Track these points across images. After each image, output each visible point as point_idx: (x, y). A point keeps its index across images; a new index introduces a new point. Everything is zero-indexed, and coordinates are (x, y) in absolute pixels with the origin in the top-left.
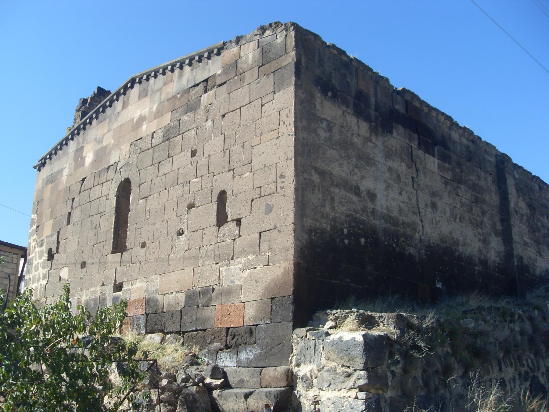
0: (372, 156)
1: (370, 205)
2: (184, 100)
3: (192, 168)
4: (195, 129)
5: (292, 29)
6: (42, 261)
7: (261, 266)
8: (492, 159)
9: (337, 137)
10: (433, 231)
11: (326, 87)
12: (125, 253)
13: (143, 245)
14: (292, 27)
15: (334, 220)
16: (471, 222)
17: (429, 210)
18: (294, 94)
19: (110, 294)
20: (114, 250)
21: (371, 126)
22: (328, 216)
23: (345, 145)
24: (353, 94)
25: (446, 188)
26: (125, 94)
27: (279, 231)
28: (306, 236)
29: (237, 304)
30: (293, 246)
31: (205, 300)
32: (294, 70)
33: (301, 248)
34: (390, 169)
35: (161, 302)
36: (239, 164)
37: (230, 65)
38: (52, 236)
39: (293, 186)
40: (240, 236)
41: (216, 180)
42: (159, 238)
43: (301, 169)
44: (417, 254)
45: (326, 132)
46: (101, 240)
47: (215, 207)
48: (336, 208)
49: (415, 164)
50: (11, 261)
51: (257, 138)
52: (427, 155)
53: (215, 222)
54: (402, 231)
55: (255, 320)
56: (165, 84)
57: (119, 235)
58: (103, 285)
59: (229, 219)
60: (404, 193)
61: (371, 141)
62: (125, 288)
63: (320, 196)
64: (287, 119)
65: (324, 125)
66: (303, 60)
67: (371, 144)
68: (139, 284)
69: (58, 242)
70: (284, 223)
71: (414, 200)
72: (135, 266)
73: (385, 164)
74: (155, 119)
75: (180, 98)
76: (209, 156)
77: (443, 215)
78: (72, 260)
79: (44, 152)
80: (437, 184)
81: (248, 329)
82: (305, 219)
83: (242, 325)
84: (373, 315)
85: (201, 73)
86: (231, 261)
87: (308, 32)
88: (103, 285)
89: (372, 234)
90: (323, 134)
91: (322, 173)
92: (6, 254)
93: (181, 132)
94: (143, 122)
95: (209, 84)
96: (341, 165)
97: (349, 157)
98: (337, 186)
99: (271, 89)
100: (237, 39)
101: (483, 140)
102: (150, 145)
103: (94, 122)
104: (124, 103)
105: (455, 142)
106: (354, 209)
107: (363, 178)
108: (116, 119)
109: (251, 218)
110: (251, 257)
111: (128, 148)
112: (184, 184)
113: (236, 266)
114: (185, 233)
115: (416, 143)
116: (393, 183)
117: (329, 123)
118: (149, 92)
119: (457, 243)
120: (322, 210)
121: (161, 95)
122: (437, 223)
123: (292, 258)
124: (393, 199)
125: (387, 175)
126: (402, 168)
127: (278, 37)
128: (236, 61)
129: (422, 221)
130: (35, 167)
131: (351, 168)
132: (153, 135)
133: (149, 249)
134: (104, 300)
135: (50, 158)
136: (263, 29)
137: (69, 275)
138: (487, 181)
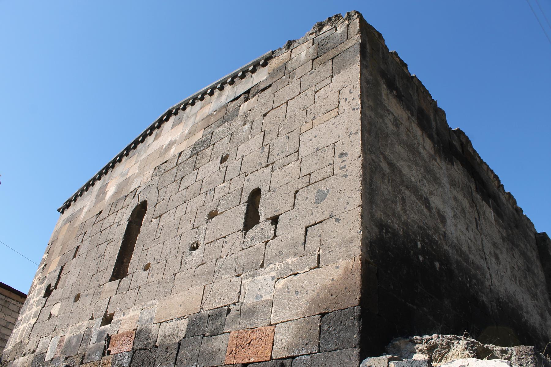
0: (438, 175)
1: (440, 226)
2: (221, 114)
3: (220, 173)
4: (230, 136)
5: (355, 17)
6: (38, 298)
7: (307, 269)
8: (533, 236)
9: (405, 138)
10: (499, 284)
11: (391, 86)
12: (124, 279)
13: (147, 267)
14: (357, 15)
15: (406, 224)
16: (528, 290)
17: (493, 260)
18: (359, 70)
19: (97, 326)
20: (114, 278)
21: (434, 147)
22: (399, 217)
23: (412, 149)
24: (416, 107)
25: (504, 244)
26: (159, 127)
27: (337, 220)
28: (376, 230)
29: (263, 328)
30: (360, 235)
31: (214, 326)
32: (359, 49)
33: (370, 242)
34: (455, 198)
35: (154, 333)
36: (281, 156)
37: (278, 69)
38: (55, 271)
39: (359, 162)
40: (275, 236)
41: (248, 181)
42: (168, 257)
43: (368, 148)
44: (490, 306)
45: (393, 124)
46: (102, 269)
47: (244, 208)
48: (408, 212)
49: (476, 206)
50: (17, 311)
51: (307, 124)
52: (484, 202)
53: (241, 226)
54: (473, 271)
55: (291, 349)
56: (201, 108)
57: (123, 263)
58: (92, 318)
59: (262, 218)
60: (469, 229)
61: (436, 161)
62: (115, 320)
63: (390, 188)
64: (350, 95)
65: (391, 117)
66: (368, 46)
67: (436, 163)
68: (133, 313)
69: (59, 277)
70: (345, 208)
71: (480, 242)
72: (132, 294)
73: (450, 191)
74: (185, 139)
75: (216, 114)
76: (243, 157)
77: (505, 271)
78: (67, 295)
79: (70, 195)
80: (497, 238)
81: (279, 364)
82: (374, 208)
83: (268, 359)
84: (491, 348)
85: (242, 87)
86: (260, 270)
87: (371, 27)
88: (92, 318)
89: (445, 260)
90: (391, 127)
91: (391, 165)
92: (13, 302)
93: (212, 143)
94: (172, 146)
95: (251, 93)
96: (409, 167)
97: (417, 165)
98: (407, 187)
99: (329, 73)
100: (288, 43)
101: (524, 214)
102: (175, 164)
103: (124, 159)
104: (157, 135)
105: (504, 204)
106: (426, 224)
107: (431, 193)
108: (145, 151)
109: (294, 212)
110: (290, 260)
111: (152, 172)
112: (208, 192)
113: (266, 277)
114: (200, 247)
115: (474, 186)
116: (460, 215)
117: (395, 120)
118: (184, 119)
119: (520, 307)
120: (393, 207)
121: (196, 117)
122: (502, 277)
123: (359, 252)
124: (462, 232)
125: (453, 203)
126: (466, 204)
127: (338, 29)
128: (286, 64)
129: (488, 268)
130: (59, 210)
131: (420, 176)
132: (180, 155)
133: (153, 271)
134: (88, 335)
135: (75, 200)
136: (321, 26)
137: (59, 311)
138: (533, 255)
